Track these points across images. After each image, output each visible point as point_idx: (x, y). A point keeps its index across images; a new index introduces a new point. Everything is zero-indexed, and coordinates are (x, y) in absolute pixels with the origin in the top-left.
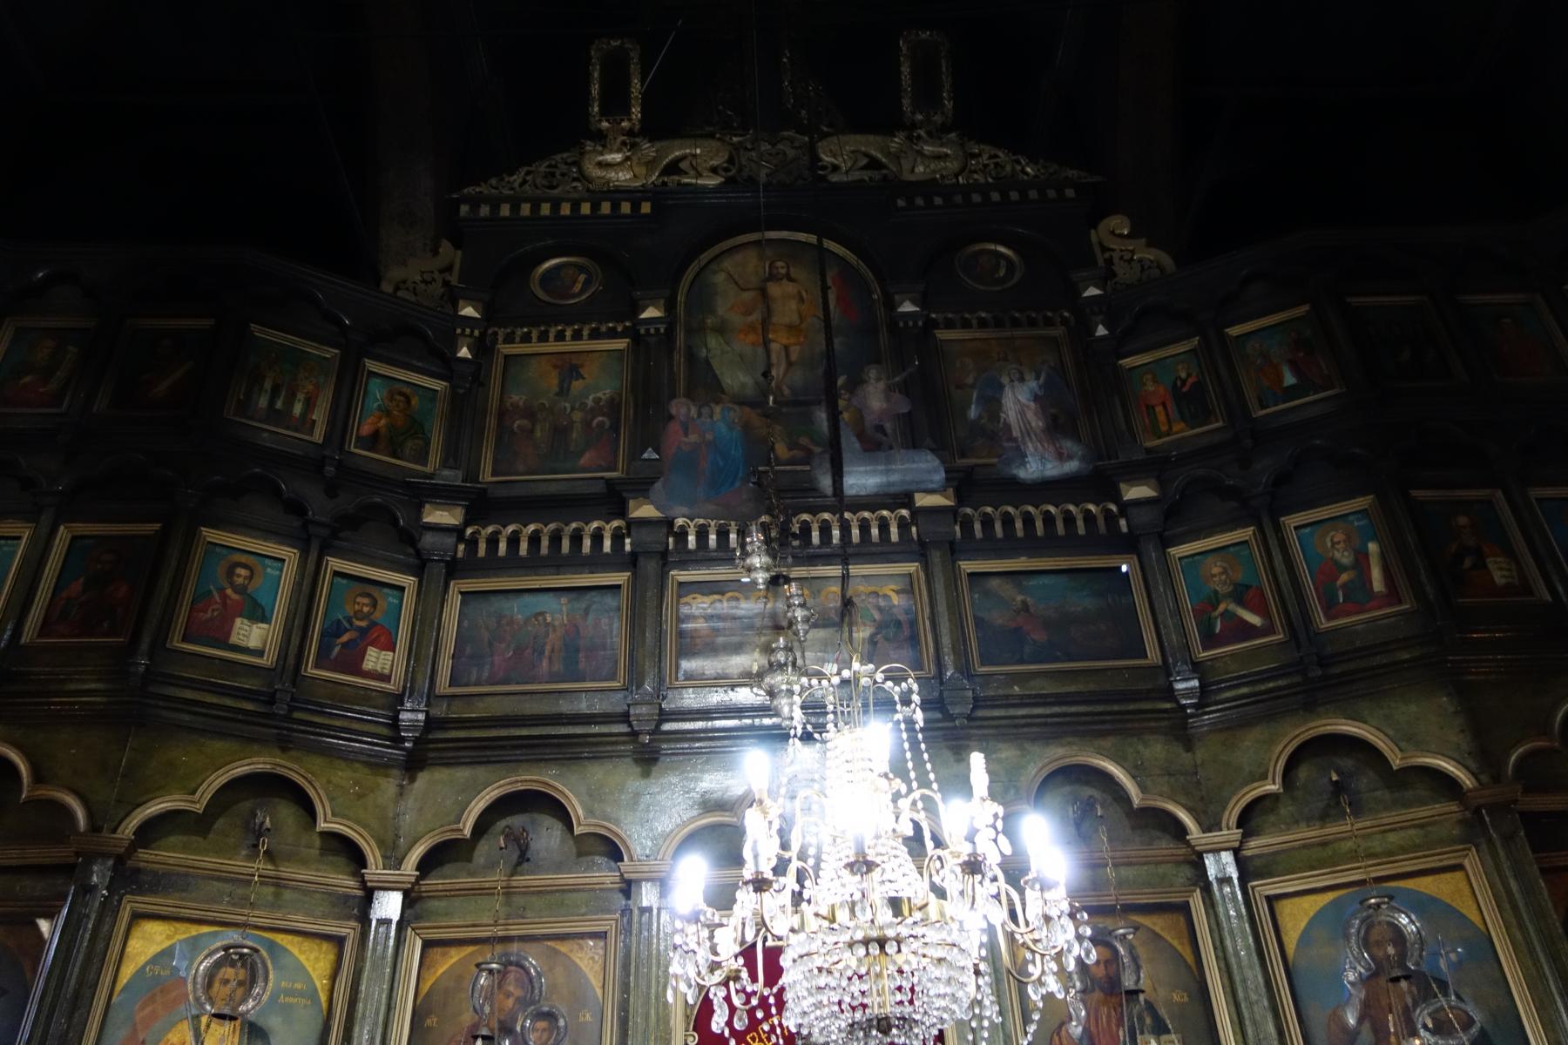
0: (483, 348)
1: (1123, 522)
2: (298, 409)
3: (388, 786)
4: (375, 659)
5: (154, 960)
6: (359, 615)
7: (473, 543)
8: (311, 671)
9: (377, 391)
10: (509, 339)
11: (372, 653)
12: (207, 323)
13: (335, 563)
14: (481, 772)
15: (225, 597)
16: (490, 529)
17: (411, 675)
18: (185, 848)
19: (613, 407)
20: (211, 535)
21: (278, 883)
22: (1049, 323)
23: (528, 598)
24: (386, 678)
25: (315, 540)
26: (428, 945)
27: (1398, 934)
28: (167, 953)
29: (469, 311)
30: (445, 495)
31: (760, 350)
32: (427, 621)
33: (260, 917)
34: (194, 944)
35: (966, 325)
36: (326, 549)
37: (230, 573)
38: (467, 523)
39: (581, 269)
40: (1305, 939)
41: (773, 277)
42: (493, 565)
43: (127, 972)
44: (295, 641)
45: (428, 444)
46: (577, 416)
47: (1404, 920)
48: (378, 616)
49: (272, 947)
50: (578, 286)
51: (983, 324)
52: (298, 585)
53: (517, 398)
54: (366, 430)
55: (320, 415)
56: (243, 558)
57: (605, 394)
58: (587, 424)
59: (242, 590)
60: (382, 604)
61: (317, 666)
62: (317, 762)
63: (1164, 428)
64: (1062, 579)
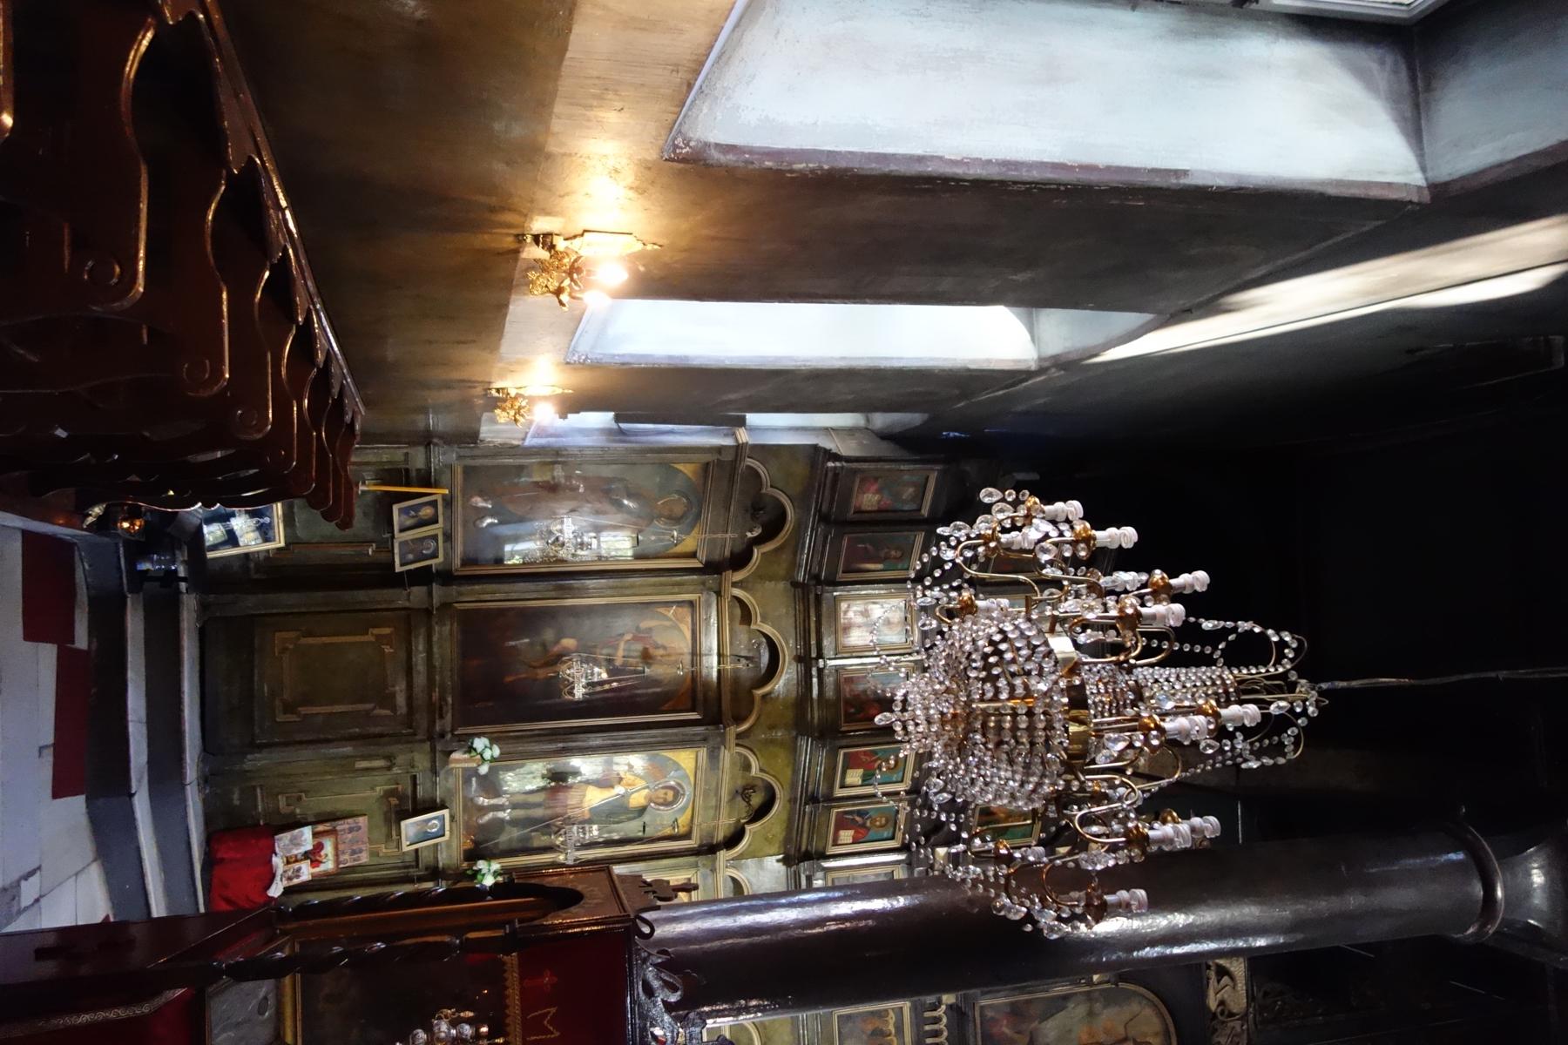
5: (675, 763)
6: (873, 821)
11: (851, 832)
28: (677, 767)
33: (699, 802)
62: (784, 816)
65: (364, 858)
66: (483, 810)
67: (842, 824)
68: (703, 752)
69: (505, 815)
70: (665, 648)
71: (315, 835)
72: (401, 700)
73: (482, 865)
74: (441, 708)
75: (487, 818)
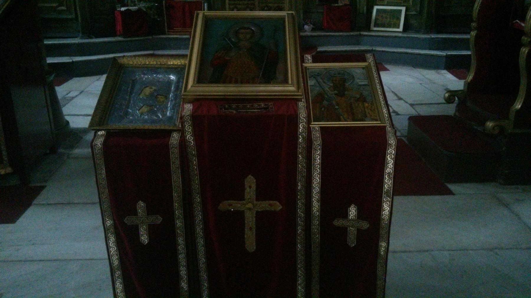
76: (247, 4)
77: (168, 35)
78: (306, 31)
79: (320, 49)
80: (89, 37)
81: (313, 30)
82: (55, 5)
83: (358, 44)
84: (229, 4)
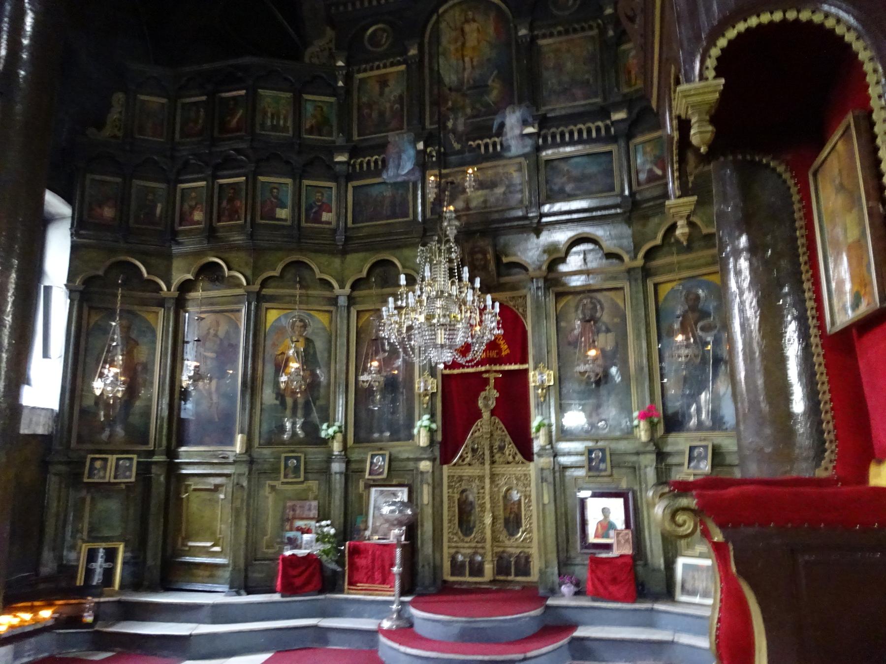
0: (348, 78)
1: (612, 130)
2: (282, 122)
3: (337, 261)
4: (325, 216)
6: (319, 201)
7: (354, 166)
8: (303, 224)
9: (310, 108)
10: (359, 72)
11: (324, 214)
12: (243, 92)
13: (306, 182)
14: (367, 254)
15: (272, 202)
16: (359, 161)
17: (338, 220)
18: (277, 287)
19: (401, 97)
20: (261, 178)
21: (308, 296)
22: (591, 28)
23: (376, 186)
24: (329, 223)
25: (298, 175)
26: (358, 312)
27: (698, 297)
28: (279, 319)
29: (340, 63)
30: (341, 150)
31: (461, 62)
32: (342, 198)
34: (286, 316)
35: (551, 35)
36: (302, 177)
37: (271, 192)
38: (351, 158)
39: (384, 30)
40: (666, 299)
41: (467, 21)
42: (361, 175)
43: (268, 325)
44: (296, 214)
45: (331, 127)
46: (388, 105)
47: (700, 292)
48: (325, 200)
49: (310, 315)
50: (384, 40)
51: (560, 33)
52: (294, 195)
53: (365, 99)
54: (308, 126)
55: (289, 123)
56: (276, 186)
57: (397, 93)
58: (392, 107)
59: (276, 198)
60: (325, 195)
61: (306, 222)
62: (312, 255)
63: (633, 81)
64: (585, 159)
65: (314, 503)
66: (294, 433)
67: (317, 219)
68: (265, 305)
69: (299, 422)
70: (209, 329)
71: (291, 530)
72: (218, 481)
73: (323, 434)
74: (223, 458)
75: (299, 431)
76: (475, 547)
77: (348, 594)
78: (563, 596)
79: (581, 632)
80: (238, 594)
81: (577, 594)
82: (209, 544)
83: (651, 624)
84: (449, 547)
